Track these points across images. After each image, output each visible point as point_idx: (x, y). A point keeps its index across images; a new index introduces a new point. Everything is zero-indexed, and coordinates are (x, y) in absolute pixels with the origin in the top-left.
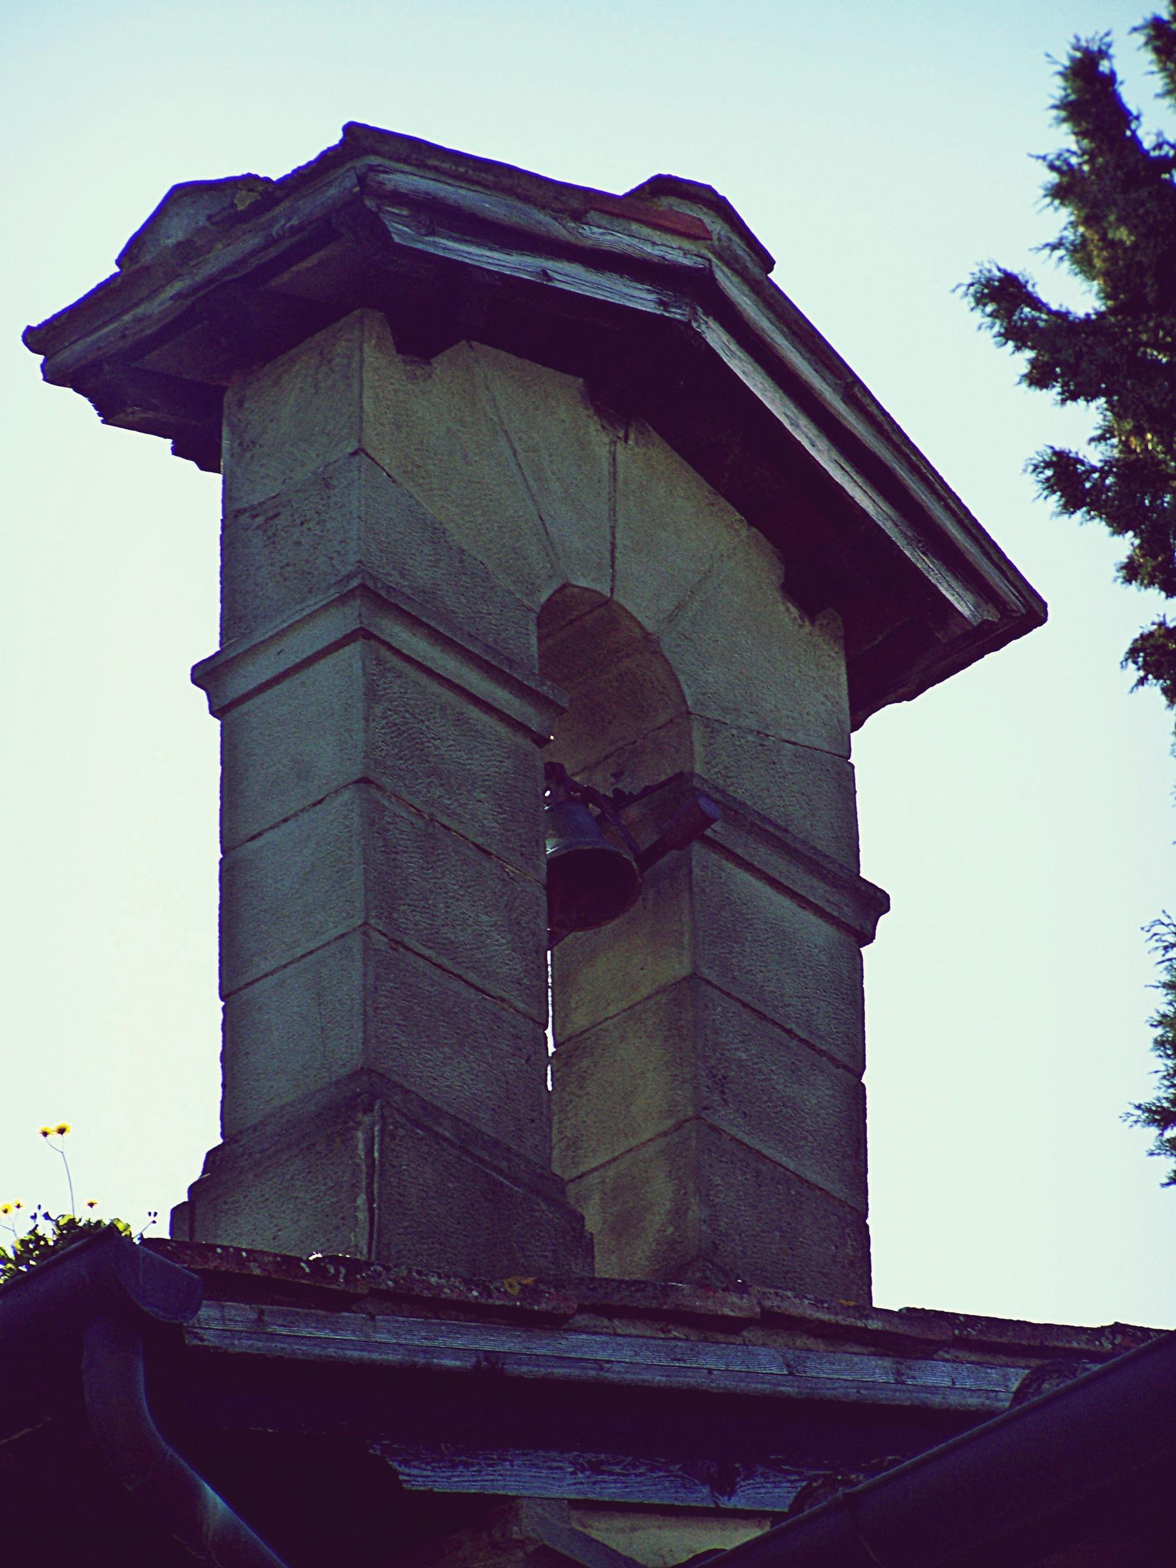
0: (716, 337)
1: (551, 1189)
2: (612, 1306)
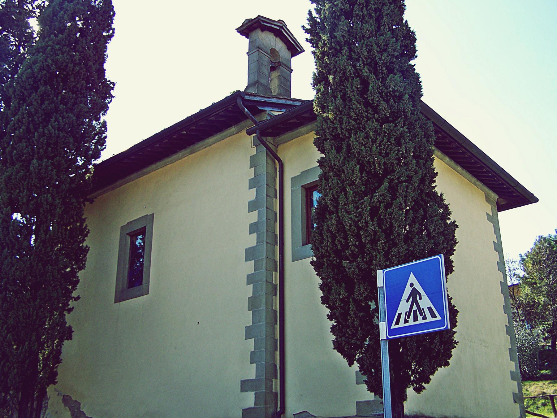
0: (283, 31)
1: (270, 89)
2: (273, 97)
